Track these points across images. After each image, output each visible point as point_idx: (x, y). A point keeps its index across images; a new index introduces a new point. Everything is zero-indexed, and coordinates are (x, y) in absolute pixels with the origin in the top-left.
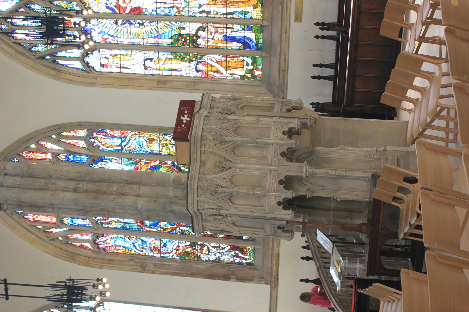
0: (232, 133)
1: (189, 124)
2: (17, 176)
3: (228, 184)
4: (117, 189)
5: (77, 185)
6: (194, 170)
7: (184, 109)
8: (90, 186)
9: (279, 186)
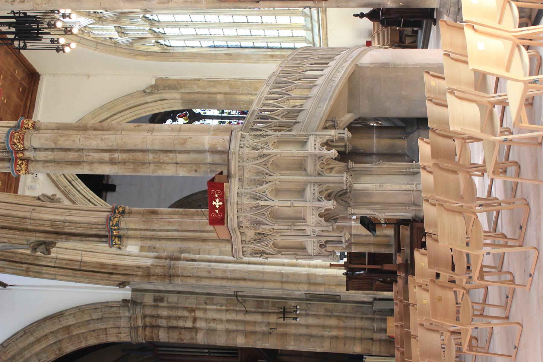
0: (268, 219)
1: (222, 209)
2: (46, 149)
3: (271, 251)
4: (153, 158)
5: (111, 155)
6: (237, 245)
7: (213, 193)
8: (125, 156)
9: (320, 250)
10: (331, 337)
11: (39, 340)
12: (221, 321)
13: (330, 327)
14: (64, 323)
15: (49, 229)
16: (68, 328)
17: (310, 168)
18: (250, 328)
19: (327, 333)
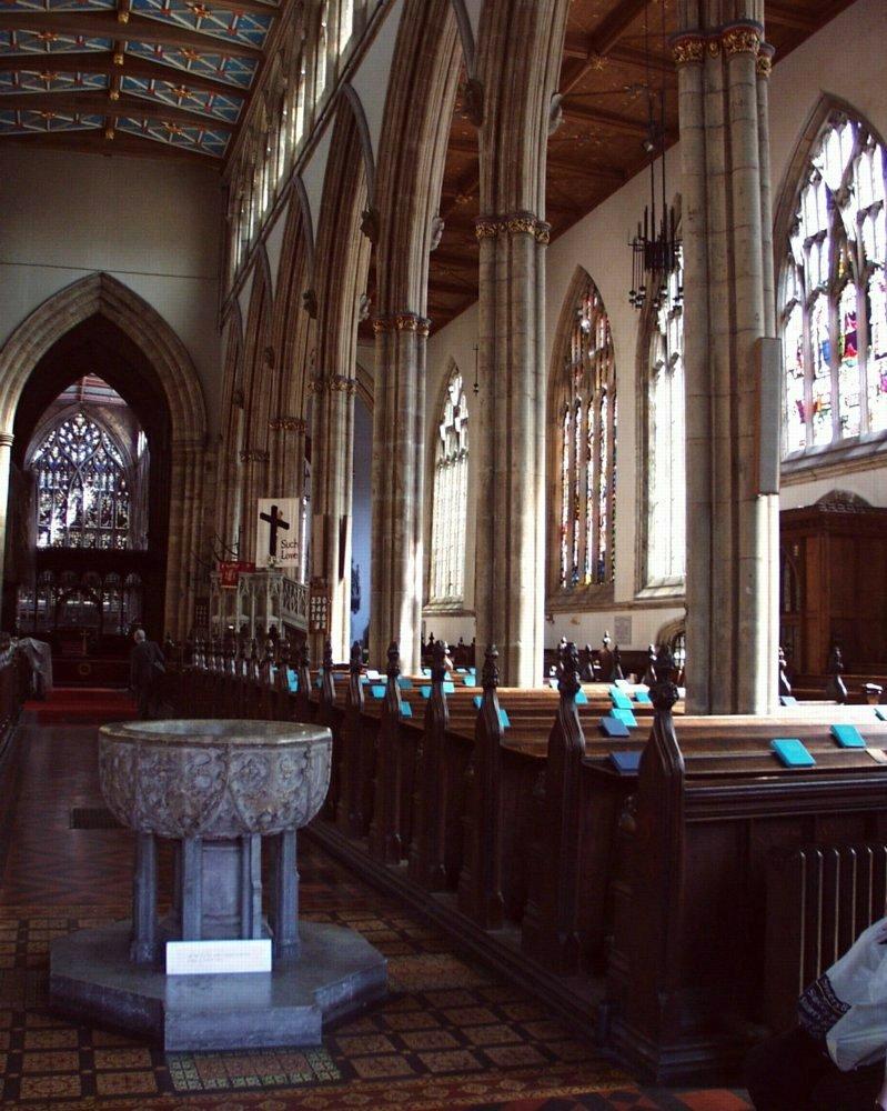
10: (177, 619)
11: (173, 359)
12: (191, 522)
13: (186, 619)
14: (188, 382)
15: (253, 404)
16: (184, 384)
17: (259, 618)
18: (184, 548)
19: (180, 616)
